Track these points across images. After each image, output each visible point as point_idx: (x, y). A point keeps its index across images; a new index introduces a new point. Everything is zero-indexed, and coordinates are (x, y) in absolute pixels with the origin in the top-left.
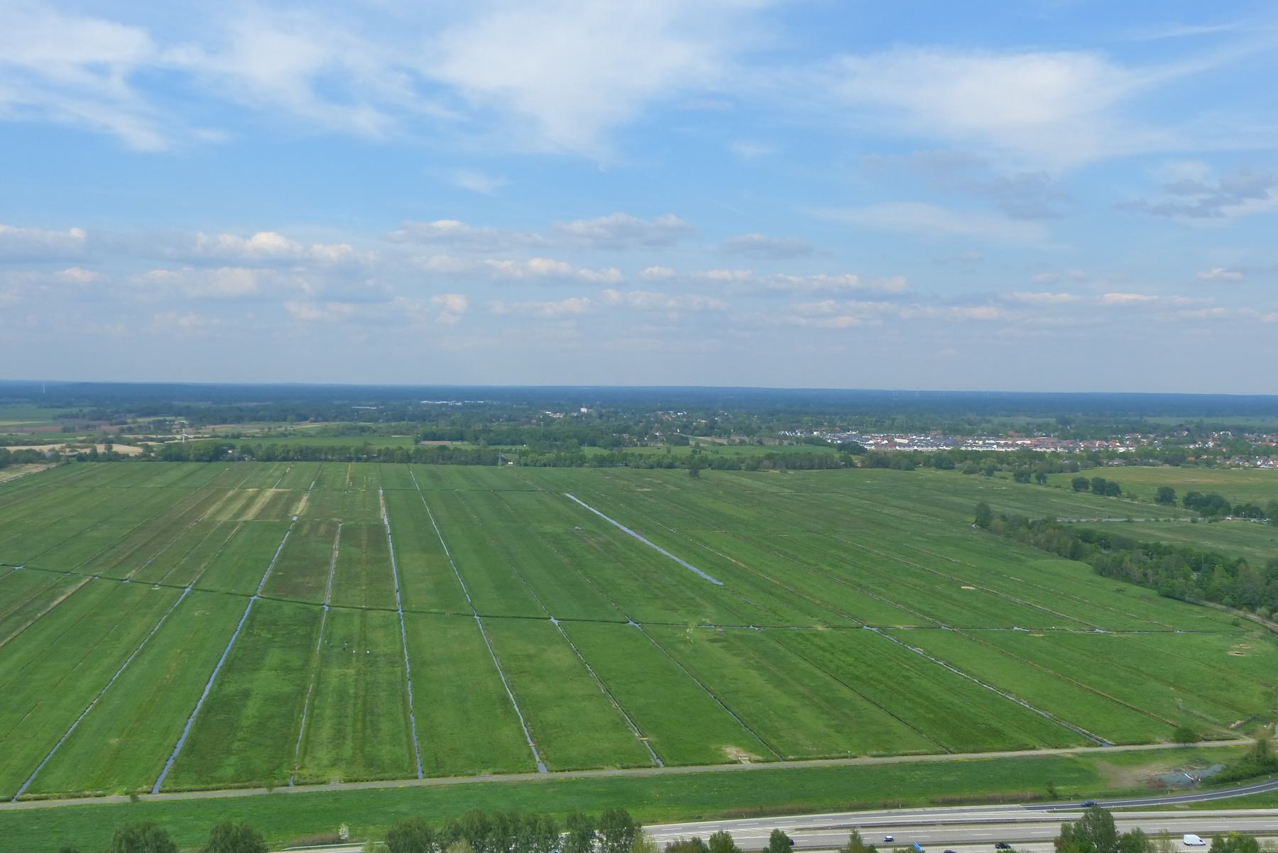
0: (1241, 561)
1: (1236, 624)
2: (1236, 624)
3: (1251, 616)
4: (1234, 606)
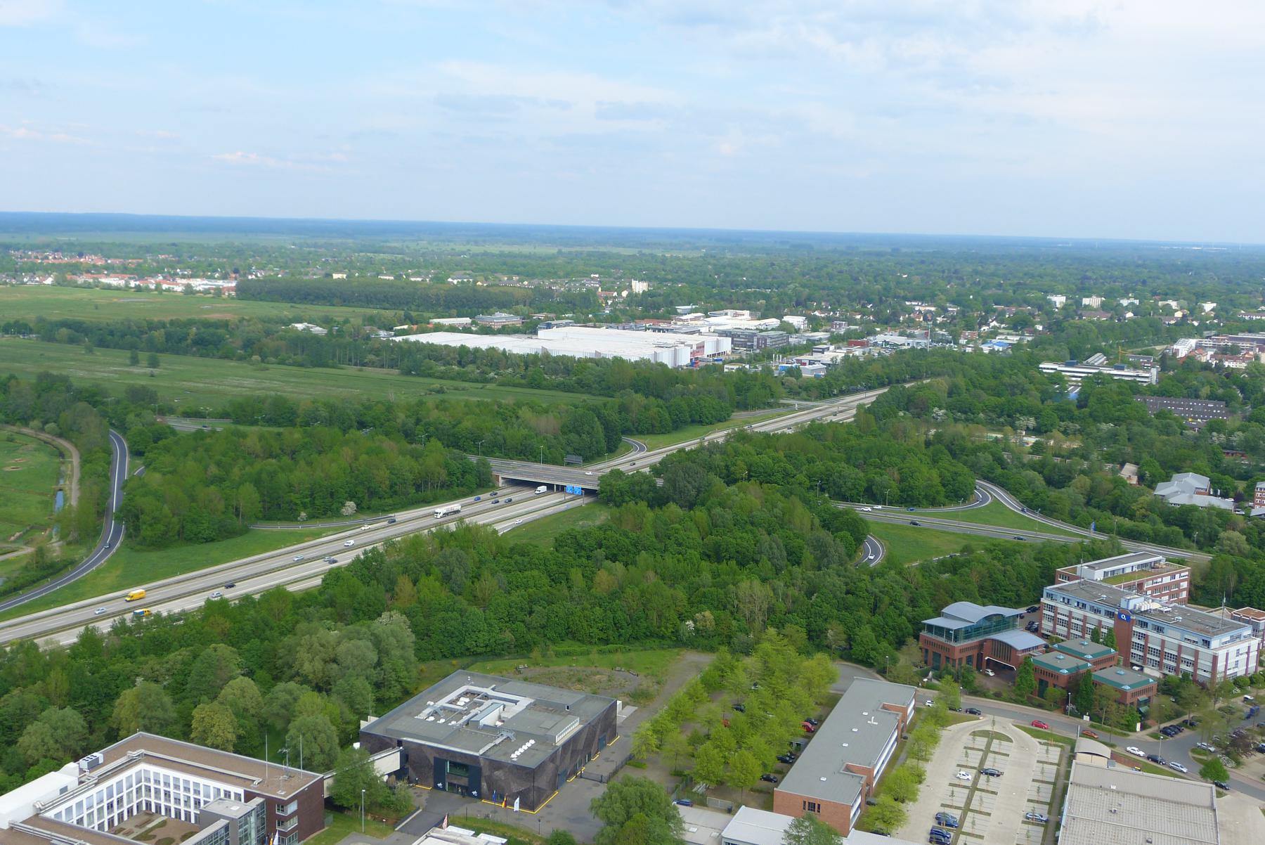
0: (12, 377)
1: (10, 440)
2: (10, 440)
3: (25, 430)
4: (7, 423)
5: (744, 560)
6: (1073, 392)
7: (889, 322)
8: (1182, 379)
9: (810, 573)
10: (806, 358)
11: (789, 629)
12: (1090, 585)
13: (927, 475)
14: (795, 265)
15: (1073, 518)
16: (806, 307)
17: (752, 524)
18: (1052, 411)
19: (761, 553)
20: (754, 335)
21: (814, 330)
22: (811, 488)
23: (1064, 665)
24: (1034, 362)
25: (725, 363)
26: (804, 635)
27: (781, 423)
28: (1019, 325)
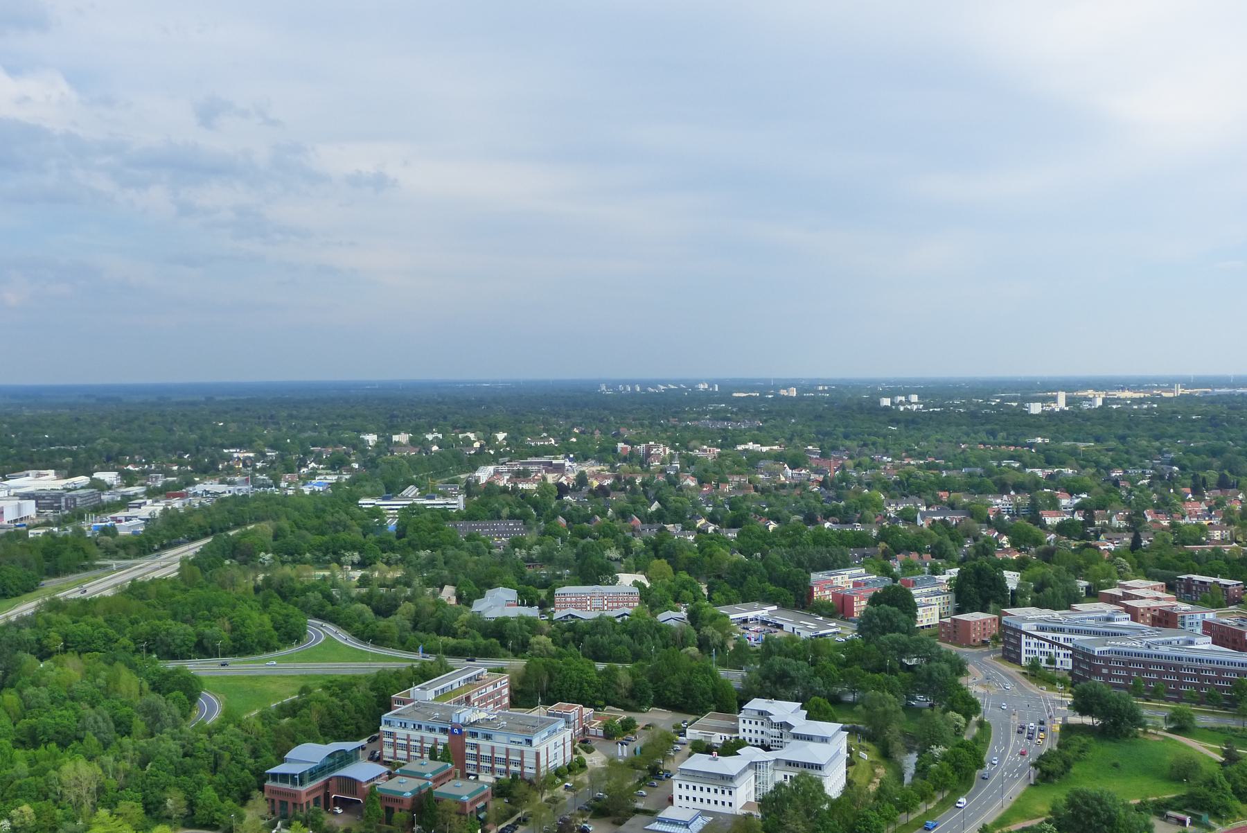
5: (65, 740)
6: (392, 524)
7: (208, 471)
8: (486, 502)
9: (142, 742)
10: (121, 514)
11: (124, 806)
12: (422, 707)
13: (258, 621)
14: (102, 418)
15: (404, 645)
16: (119, 462)
17: (73, 699)
18: (375, 545)
19: (84, 729)
20: (62, 495)
21: (128, 485)
22: (137, 651)
23: (406, 787)
24: (353, 499)
25: (29, 528)
26: (140, 810)
27: (102, 585)
28: (337, 464)
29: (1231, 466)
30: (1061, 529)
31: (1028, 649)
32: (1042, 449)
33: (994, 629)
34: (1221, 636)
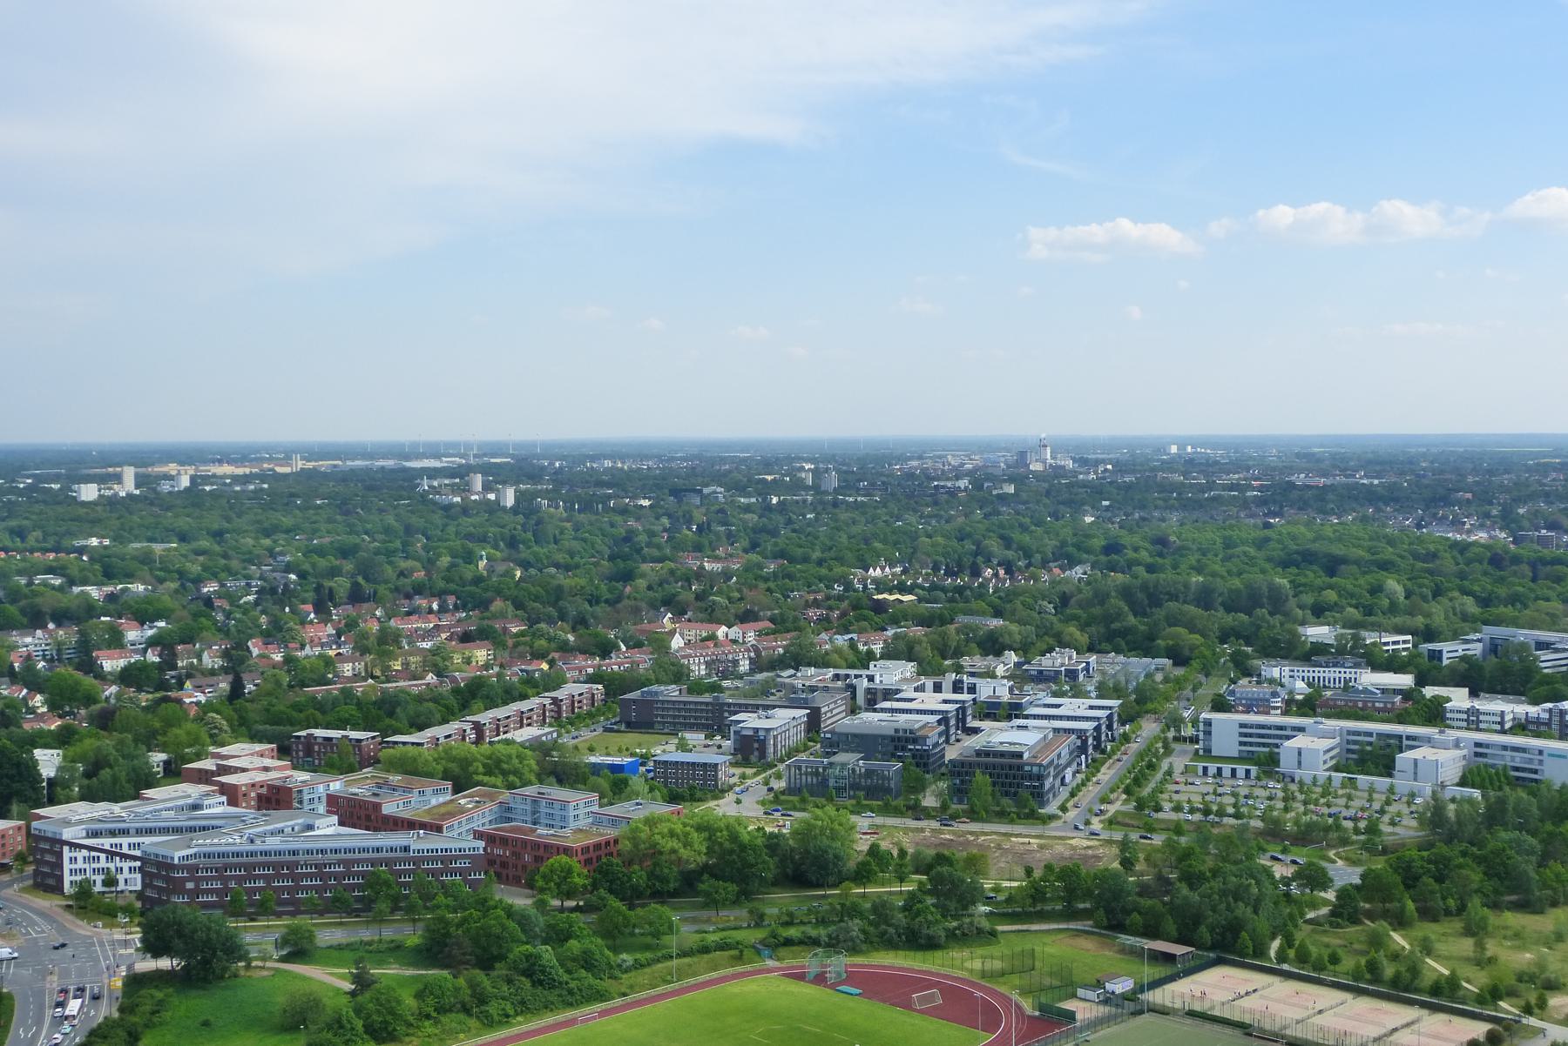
29: (366, 570)
30: (127, 677)
31: (74, 867)
32: (98, 556)
33: (19, 843)
34: (353, 813)
